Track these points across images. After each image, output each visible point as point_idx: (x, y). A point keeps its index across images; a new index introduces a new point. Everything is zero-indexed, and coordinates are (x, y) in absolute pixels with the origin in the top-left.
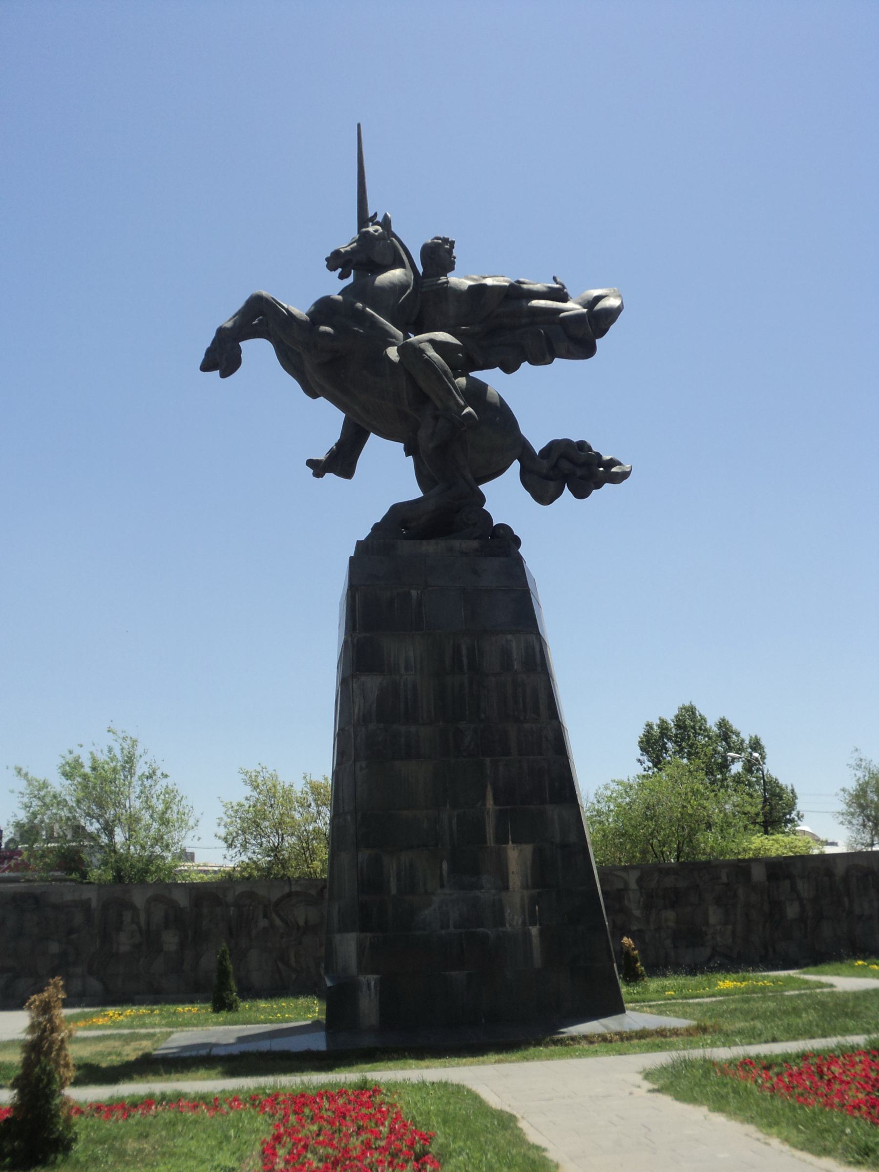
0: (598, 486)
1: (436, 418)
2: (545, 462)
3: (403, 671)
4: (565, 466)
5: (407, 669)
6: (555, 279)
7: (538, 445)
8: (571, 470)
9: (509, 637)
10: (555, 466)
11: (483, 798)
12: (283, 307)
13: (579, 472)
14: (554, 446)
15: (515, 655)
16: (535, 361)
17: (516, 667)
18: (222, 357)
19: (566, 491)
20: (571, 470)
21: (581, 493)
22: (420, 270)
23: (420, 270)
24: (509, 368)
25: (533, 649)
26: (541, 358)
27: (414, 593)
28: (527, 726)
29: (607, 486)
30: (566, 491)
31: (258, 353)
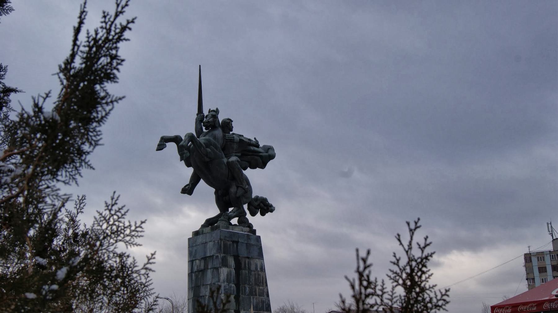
0: (267, 212)
1: (238, 187)
6: (255, 139)
7: (253, 196)
8: (263, 207)
10: (259, 205)
11: (250, 308)
13: (265, 208)
14: (257, 198)
16: (251, 168)
18: (161, 147)
20: (263, 207)
21: (263, 214)
24: (245, 169)
26: (253, 167)
28: (261, 288)
29: (269, 213)
31: (172, 147)
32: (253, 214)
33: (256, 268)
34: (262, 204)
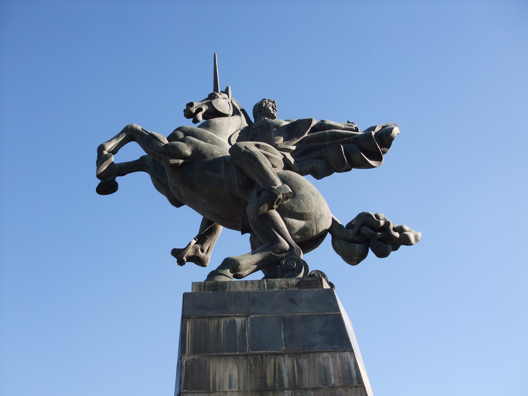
0: (396, 248)
2: (351, 230)
3: (227, 388)
4: (366, 230)
5: (230, 386)
9: (325, 355)
10: (359, 233)
12: (148, 132)
15: (332, 372)
17: (333, 381)
19: (371, 253)
21: (382, 254)
22: (253, 120)
23: (253, 120)
25: (349, 365)
27: (238, 320)
29: (402, 247)
30: (370, 252)
32: (353, 258)
33: (326, 380)
34: (366, 230)
